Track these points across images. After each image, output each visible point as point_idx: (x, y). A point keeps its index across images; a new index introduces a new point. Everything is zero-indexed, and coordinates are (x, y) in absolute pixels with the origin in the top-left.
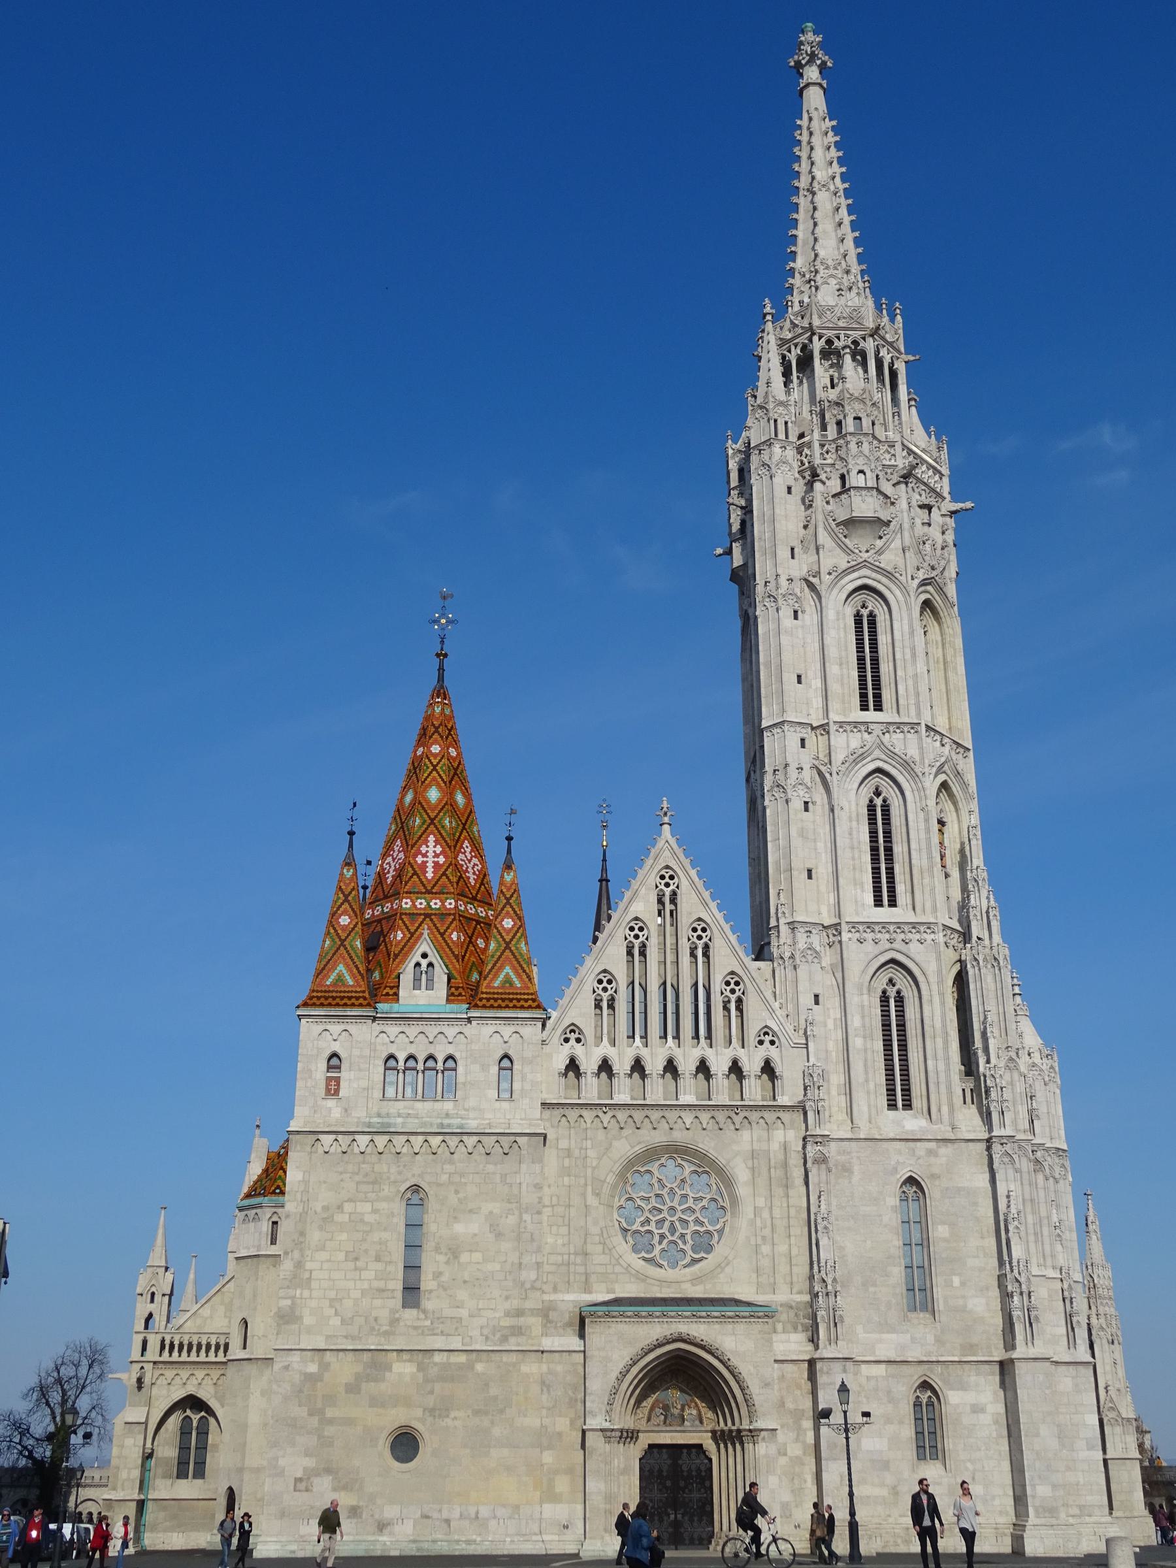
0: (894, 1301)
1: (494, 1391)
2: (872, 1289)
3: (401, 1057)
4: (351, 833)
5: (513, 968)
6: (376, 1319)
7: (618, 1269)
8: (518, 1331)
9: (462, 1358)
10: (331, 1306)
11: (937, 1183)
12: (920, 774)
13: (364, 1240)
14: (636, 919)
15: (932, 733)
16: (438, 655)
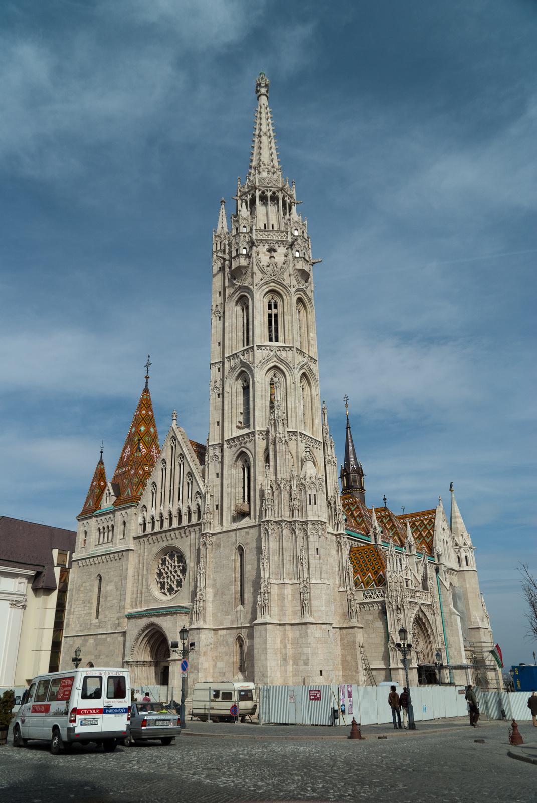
0: (231, 601)
1: (111, 648)
2: (224, 597)
3: (101, 528)
4: (102, 452)
5: (131, 488)
6: (87, 624)
7: (151, 598)
8: (118, 625)
9: (104, 637)
10: (78, 620)
11: (248, 546)
12: (253, 368)
13: (86, 596)
14: (164, 460)
15: (263, 348)
16: (146, 377)
